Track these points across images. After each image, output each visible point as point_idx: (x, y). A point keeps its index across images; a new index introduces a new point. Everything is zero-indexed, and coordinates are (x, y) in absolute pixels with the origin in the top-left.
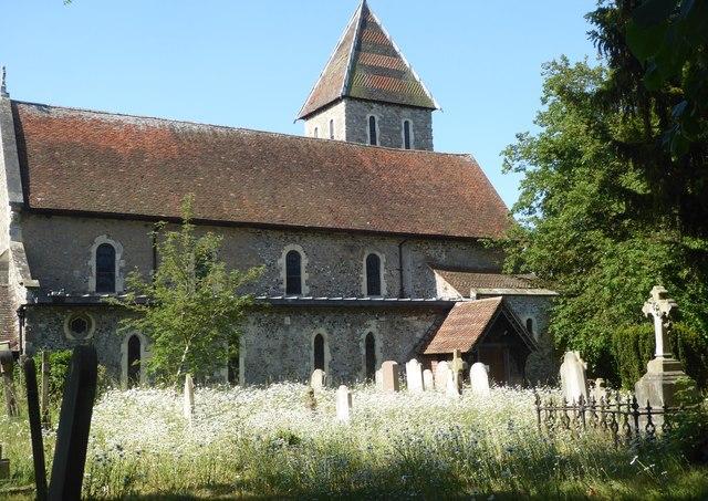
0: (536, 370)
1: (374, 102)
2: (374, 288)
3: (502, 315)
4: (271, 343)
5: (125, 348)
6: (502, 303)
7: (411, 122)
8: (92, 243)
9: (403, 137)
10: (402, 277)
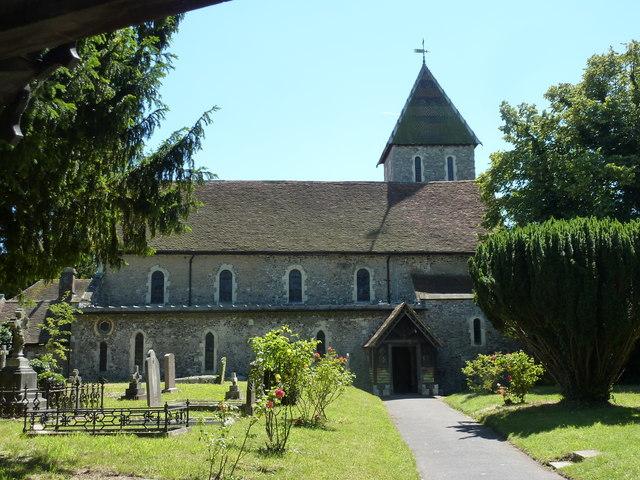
5: (133, 341)
9: (414, 170)
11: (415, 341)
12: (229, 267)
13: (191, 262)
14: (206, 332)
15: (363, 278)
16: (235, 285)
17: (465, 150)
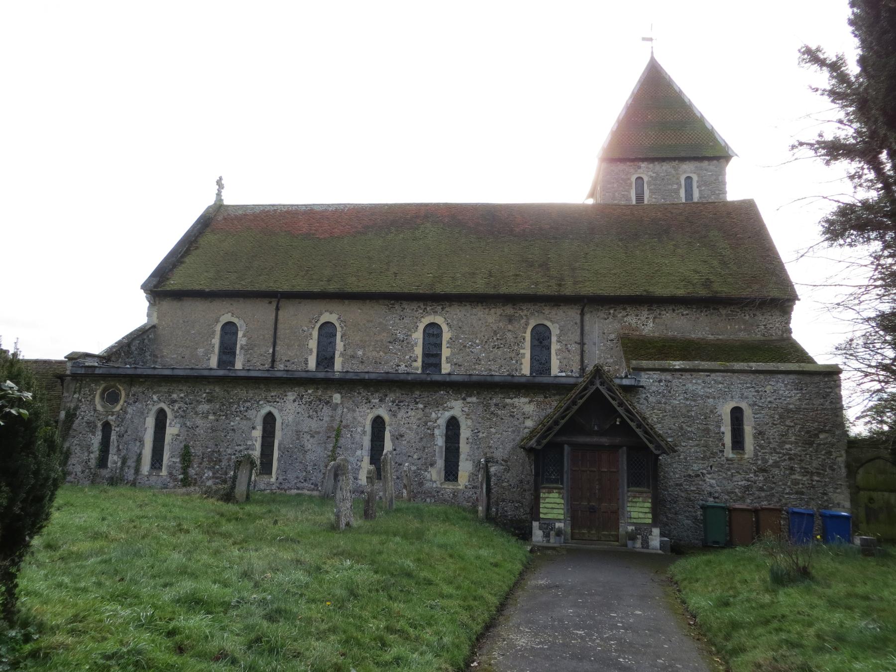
0: (747, 488)
4: (314, 424)
5: (150, 422)
7: (695, 178)
8: (217, 321)
10: (582, 352)
11: (617, 440)
12: (333, 318)
13: (277, 309)
14: (264, 411)
15: (541, 339)
16: (340, 346)
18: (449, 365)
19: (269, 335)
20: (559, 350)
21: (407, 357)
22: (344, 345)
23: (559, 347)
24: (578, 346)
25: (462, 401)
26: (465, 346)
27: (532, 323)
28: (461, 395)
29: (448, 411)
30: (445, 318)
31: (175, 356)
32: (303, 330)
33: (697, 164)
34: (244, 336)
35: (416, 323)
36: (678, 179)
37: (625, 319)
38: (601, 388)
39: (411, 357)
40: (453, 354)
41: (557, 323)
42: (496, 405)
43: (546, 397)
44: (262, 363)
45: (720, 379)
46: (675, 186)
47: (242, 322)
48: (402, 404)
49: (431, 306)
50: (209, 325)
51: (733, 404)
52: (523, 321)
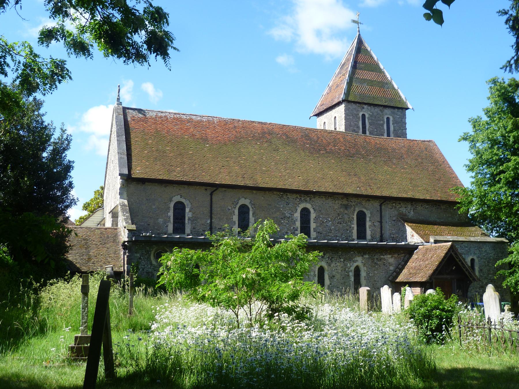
1: (365, 104)
2: (362, 235)
3: (451, 256)
6: (452, 247)
8: (171, 201)
12: (247, 202)
13: (211, 194)
17: (399, 112)
18: (315, 233)
19: (207, 211)
20: (370, 225)
21: (292, 228)
22: (255, 220)
23: (370, 224)
24: (379, 223)
25: (361, 257)
26: (323, 222)
27: (357, 210)
28: (361, 254)
29: (355, 262)
30: (312, 205)
31: (143, 224)
32: (228, 209)
33: (392, 110)
34: (190, 211)
35: (296, 207)
36: (383, 118)
37: (400, 209)
38: (453, 253)
39: (294, 228)
40: (317, 227)
41: (369, 210)
42: (377, 259)
43: (398, 255)
44: (204, 230)
45: (466, 245)
46: (382, 122)
47: (188, 202)
48: (333, 259)
49: (304, 197)
50: (165, 203)
51: (471, 257)
52: (352, 208)
